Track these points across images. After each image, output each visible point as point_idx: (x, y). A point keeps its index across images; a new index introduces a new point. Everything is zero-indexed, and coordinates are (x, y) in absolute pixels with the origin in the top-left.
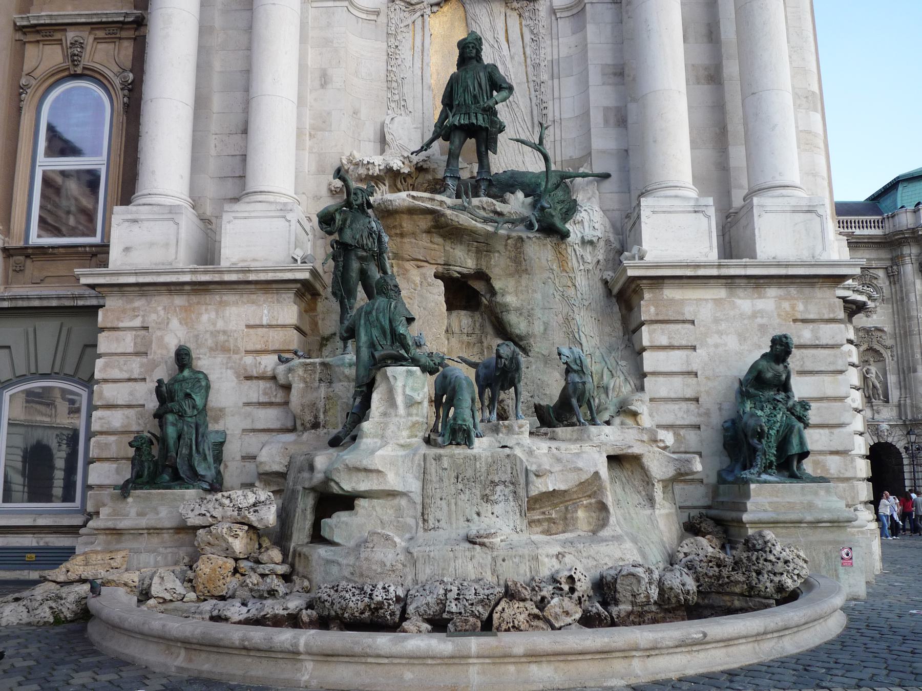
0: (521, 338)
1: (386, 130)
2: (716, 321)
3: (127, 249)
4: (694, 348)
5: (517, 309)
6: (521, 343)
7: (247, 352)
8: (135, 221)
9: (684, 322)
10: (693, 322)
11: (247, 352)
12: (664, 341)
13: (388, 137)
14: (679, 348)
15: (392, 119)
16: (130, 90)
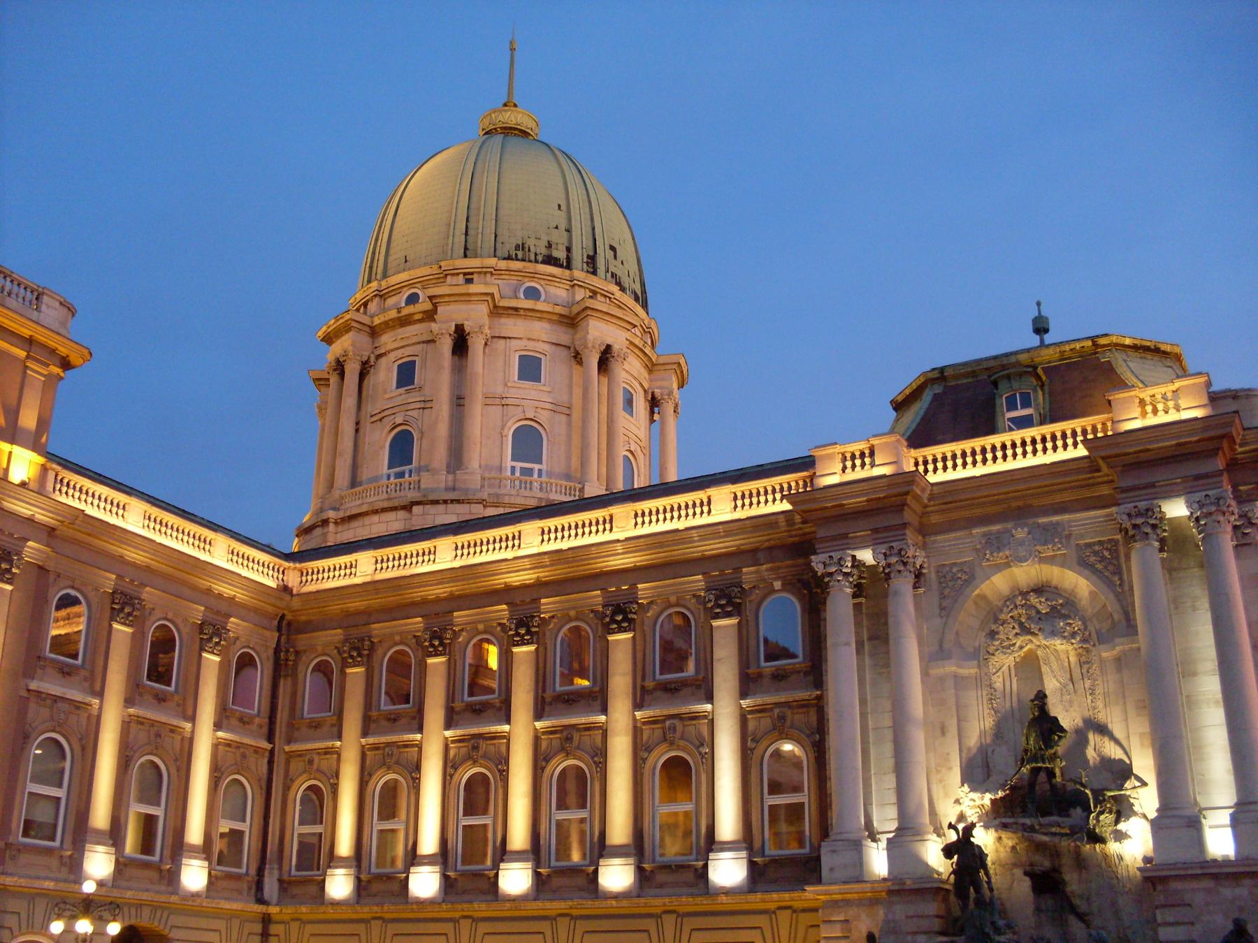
0: (1086, 914)
1: (989, 760)
2: (1208, 904)
3: (832, 870)
4: (1192, 924)
5: (1079, 896)
6: (1086, 918)
7: (908, 933)
8: (834, 851)
9: (1185, 905)
10: (1189, 905)
11: (908, 933)
12: (1171, 919)
13: (991, 765)
14: (1183, 924)
15: (993, 751)
16: (817, 747)
